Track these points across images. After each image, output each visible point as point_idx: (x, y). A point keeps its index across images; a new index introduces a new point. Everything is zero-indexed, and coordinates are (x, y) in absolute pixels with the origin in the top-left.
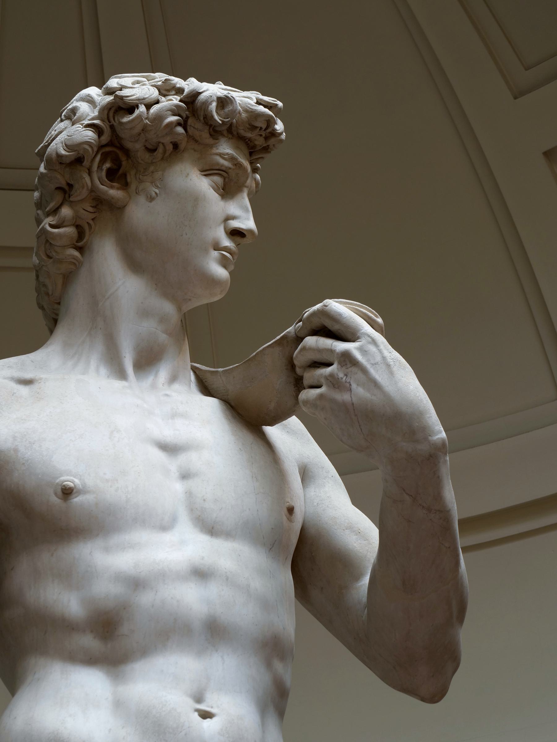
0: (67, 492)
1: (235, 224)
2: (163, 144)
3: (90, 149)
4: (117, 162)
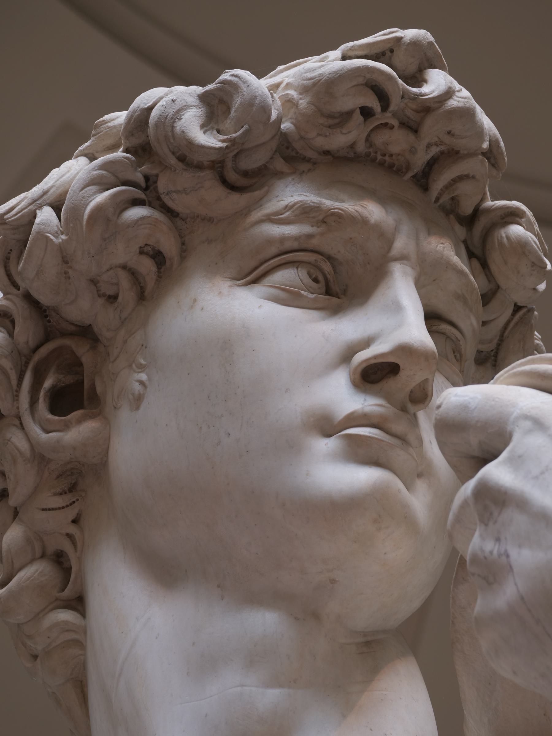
2: (124, 267)
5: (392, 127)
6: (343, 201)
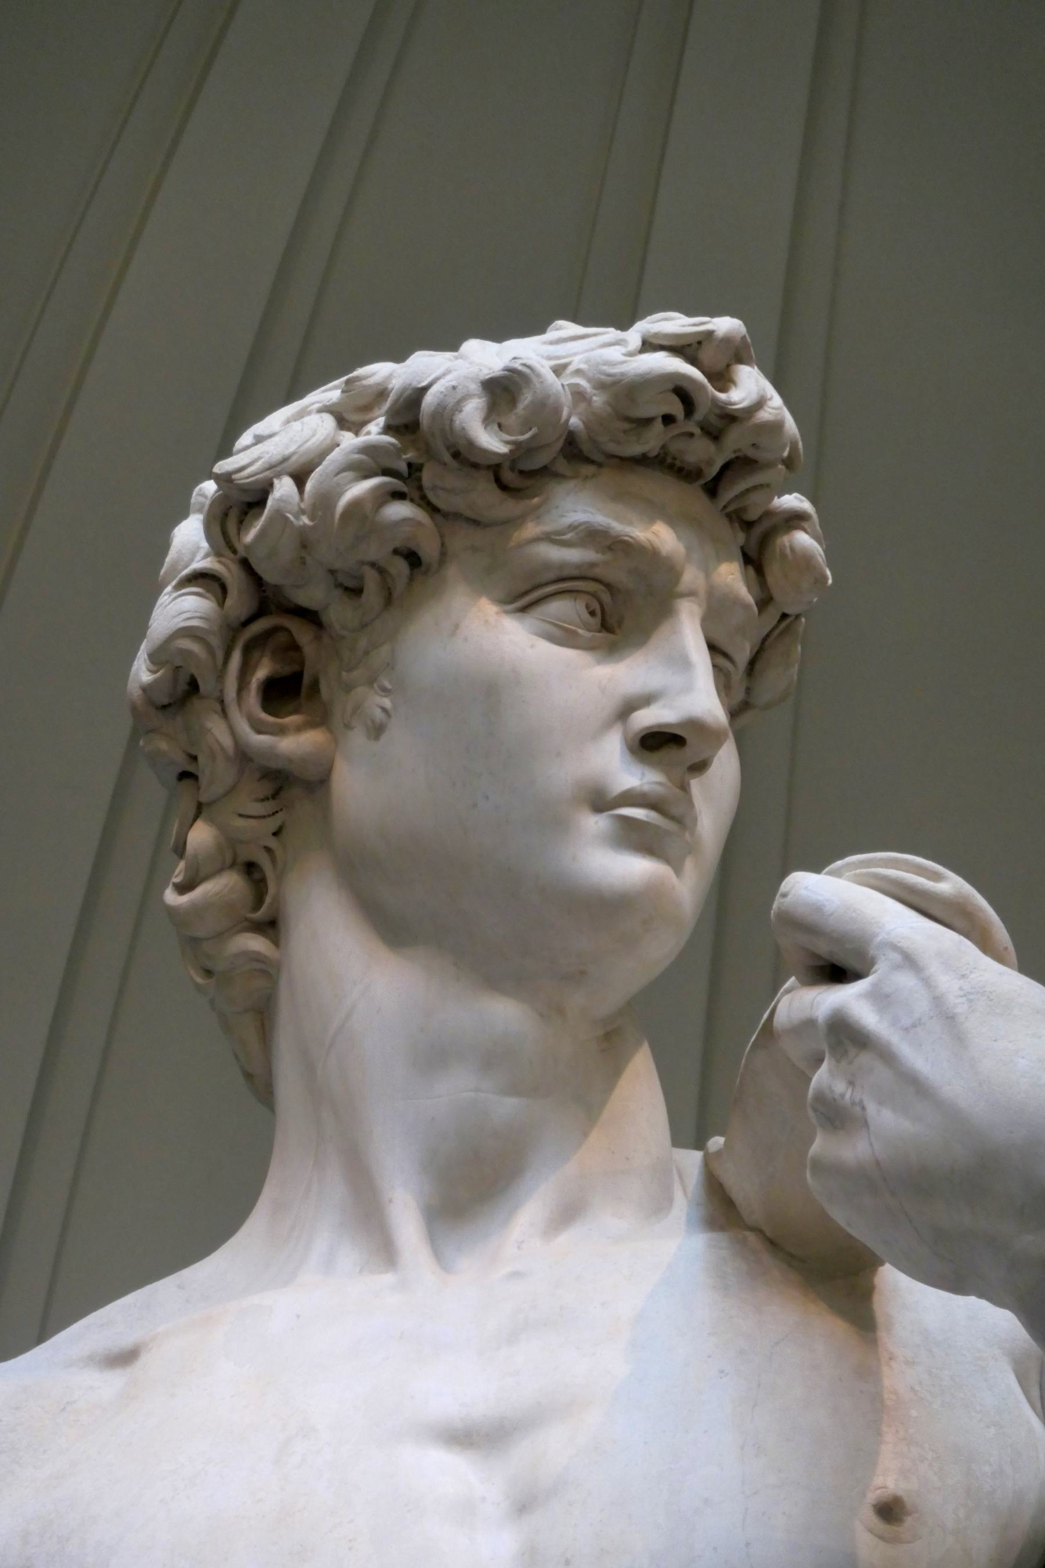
1: (647, 718)
2: (373, 565)
3: (195, 647)
5: (691, 435)
6: (630, 523)
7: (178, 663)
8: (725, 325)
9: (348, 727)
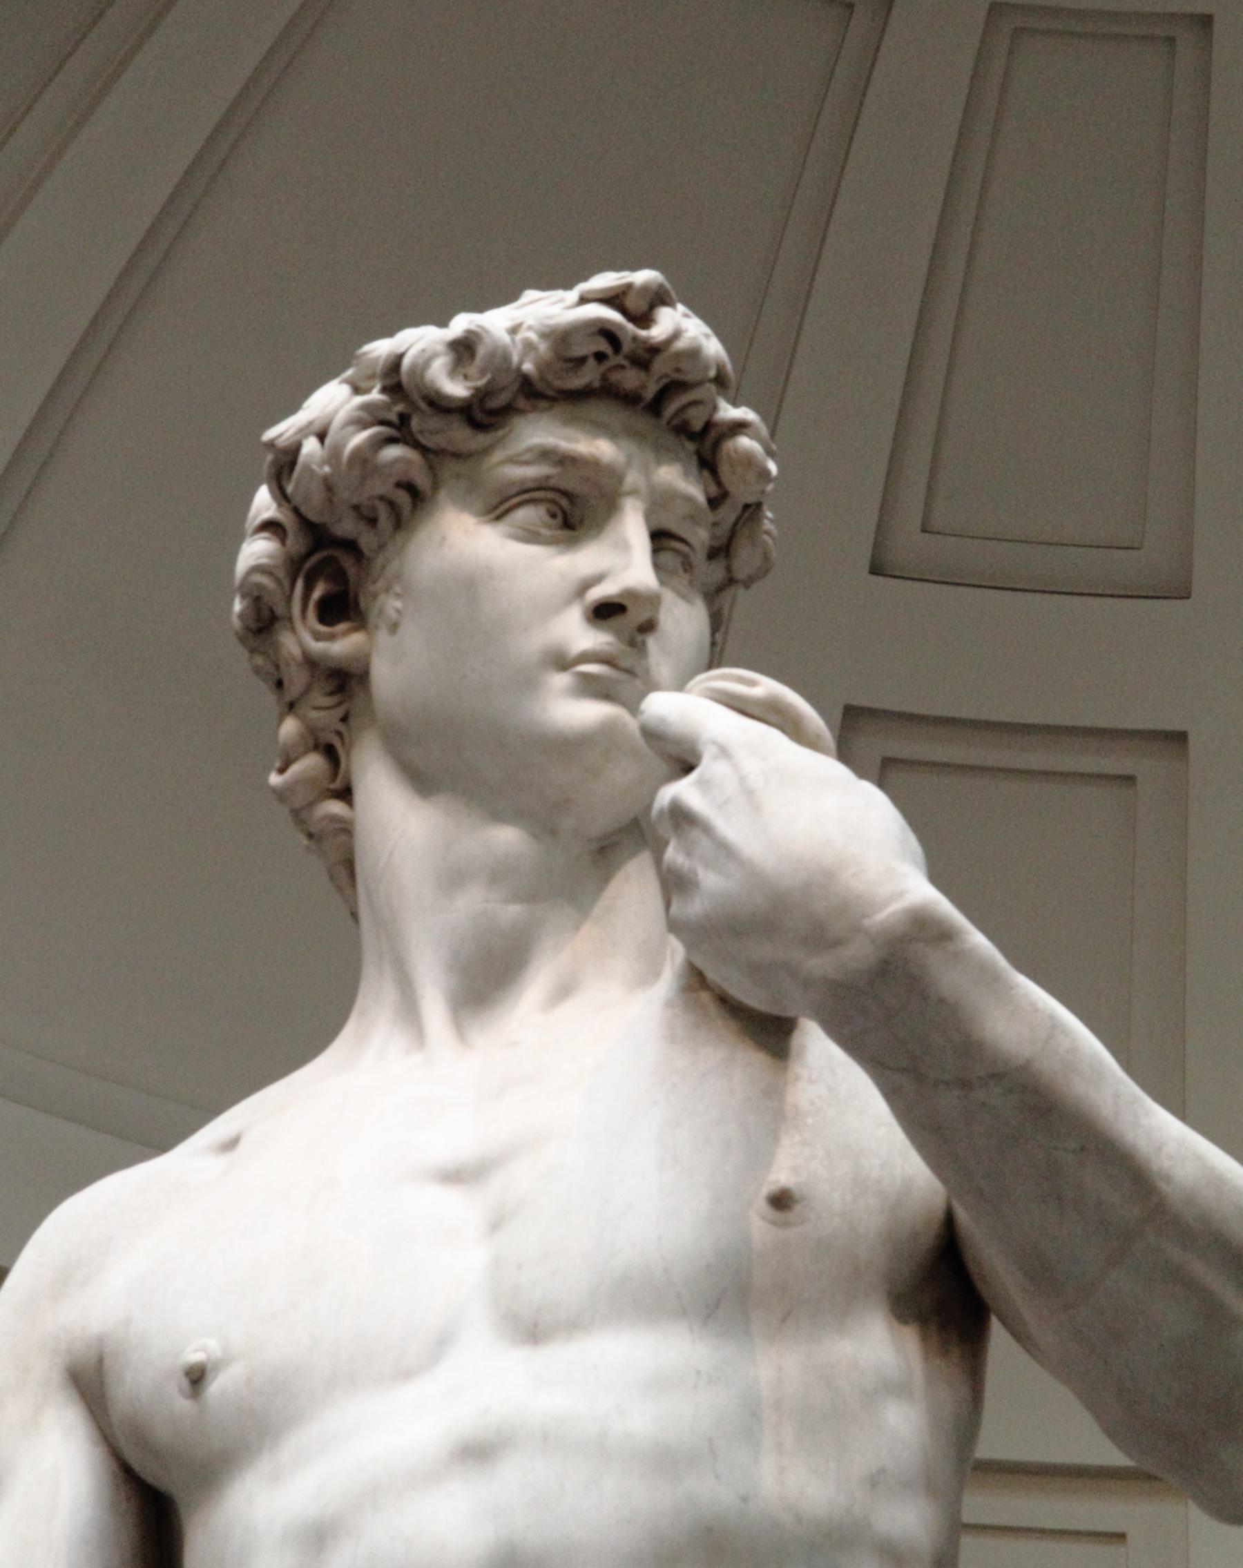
0: (197, 1377)
1: (597, 593)
2: (382, 498)
4: (339, 576)
5: (622, 367)
6: (578, 441)
7: (256, 593)
8: (644, 276)
9: (377, 627)
